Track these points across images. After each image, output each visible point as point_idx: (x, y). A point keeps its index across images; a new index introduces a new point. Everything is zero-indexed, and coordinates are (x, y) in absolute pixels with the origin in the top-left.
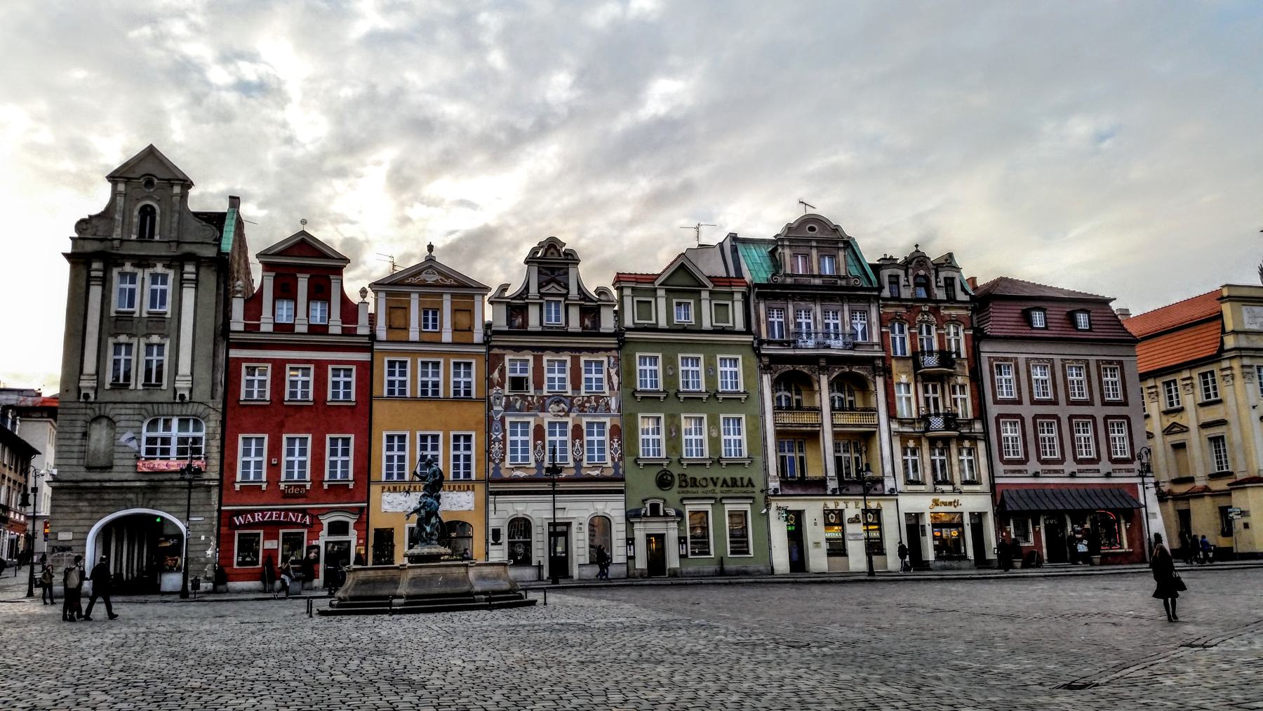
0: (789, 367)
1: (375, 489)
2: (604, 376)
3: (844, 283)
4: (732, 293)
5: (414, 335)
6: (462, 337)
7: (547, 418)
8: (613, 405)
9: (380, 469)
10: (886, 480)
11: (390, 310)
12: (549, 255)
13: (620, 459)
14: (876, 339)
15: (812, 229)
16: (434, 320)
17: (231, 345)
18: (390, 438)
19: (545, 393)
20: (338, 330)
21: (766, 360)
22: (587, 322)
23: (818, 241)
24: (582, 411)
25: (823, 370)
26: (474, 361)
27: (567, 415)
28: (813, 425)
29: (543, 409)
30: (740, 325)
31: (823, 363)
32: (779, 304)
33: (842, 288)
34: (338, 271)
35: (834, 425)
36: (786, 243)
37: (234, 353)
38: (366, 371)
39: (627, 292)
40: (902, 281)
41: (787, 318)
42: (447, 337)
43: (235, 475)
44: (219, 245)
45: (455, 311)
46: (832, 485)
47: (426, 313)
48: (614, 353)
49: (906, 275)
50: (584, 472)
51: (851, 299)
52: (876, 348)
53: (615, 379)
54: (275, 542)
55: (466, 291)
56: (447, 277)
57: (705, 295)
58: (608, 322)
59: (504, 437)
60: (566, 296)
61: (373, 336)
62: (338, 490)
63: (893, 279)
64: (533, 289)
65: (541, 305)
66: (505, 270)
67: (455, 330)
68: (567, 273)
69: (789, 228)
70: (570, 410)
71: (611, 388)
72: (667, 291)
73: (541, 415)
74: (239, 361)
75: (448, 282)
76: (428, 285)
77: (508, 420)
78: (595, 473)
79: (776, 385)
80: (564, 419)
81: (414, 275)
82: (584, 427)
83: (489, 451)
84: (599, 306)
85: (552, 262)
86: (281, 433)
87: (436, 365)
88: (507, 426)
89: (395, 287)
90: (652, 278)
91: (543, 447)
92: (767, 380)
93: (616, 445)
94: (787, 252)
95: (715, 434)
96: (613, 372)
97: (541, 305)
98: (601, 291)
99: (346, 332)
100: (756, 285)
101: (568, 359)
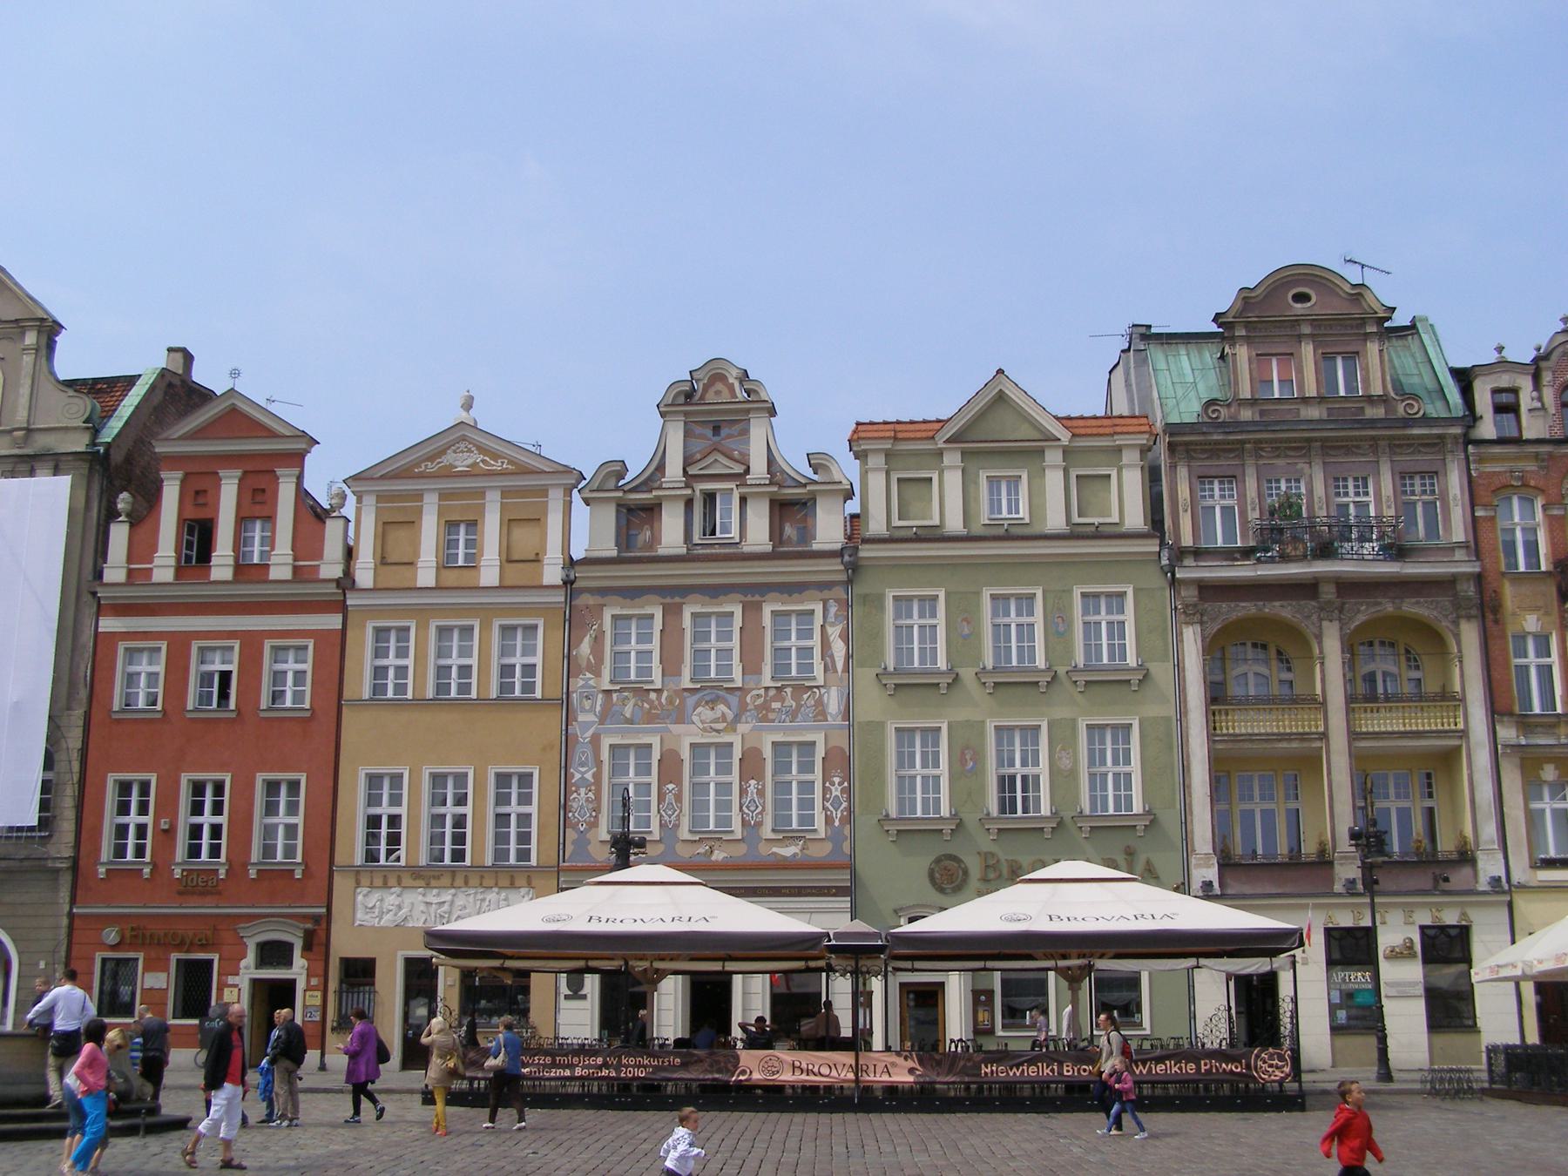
0: (1247, 608)
1: (341, 884)
2: (816, 641)
3: (1378, 412)
4: (1119, 450)
5: (426, 576)
6: (517, 574)
7: (686, 736)
8: (833, 702)
9: (352, 846)
10: (1480, 856)
11: (385, 528)
12: (710, 397)
13: (849, 817)
14: (1459, 533)
15: (1301, 298)
16: (470, 544)
17: (100, 611)
18: (374, 781)
19: (686, 683)
20: (285, 573)
21: (1190, 594)
22: (789, 531)
23: (1315, 323)
24: (765, 719)
25: (1326, 610)
26: (541, 623)
27: (731, 727)
28: (1302, 737)
29: (681, 718)
30: (1135, 518)
31: (1328, 593)
32: (1225, 463)
33: (1373, 423)
34: (296, 459)
35: (1353, 735)
36: (1240, 332)
37: (108, 624)
38: (334, 651)
39: (877, 461)
40: (1526, 399)
41: (1242, 497)
42: (489, 575)
43: (98, 850)
44: (96, 432)
45: (509, 523)
46: (1348, 871)
47: (452, 526)
48: (839, 592)
49: (1537, 384)
50: (764, 850)
51: (1397, 446)
52: (1460, 555)
53: (839, 649)
54: (163, 976)
55: (529, 482)
56: (496, 456)
57: (1054, 457)
58: (829, 529)
59: (598, 777)
60: (740, 478)
61: (347, 582)
62: (275, 879)
63: (1505, 398)
64: (674, 469)
65: (689, 503)
66: (626, 430)
67: (508, 559)
68: (745, 432)
69: (1246, 298)
70: (737, 719)
71: (829, 668)
72: (964, 453)
73: (676, 729)
74: (114, 637)
75: (497, 466)
76: (449, 473)
77: (606, 742)
78: (788, 851)
79: (1215, 650)
80: (726, 738)
81: (431, 458)
82: (768, 753)
83: (565, 807)
84: (813, 493)
85: (713, 407)
87: (467, 631)
88: (605, 755)
89: (396, 482)
90: (928, 429)
91: (679, 798)
92: (1191, 642)
93: (836, 791)
94: (1242, 353)
95: (1065, 763)
96: (834, 632)
97: (689, 503)
98: (818, 462)
99: (300, 574)
100: (1172, 429)
101: (738, 611)
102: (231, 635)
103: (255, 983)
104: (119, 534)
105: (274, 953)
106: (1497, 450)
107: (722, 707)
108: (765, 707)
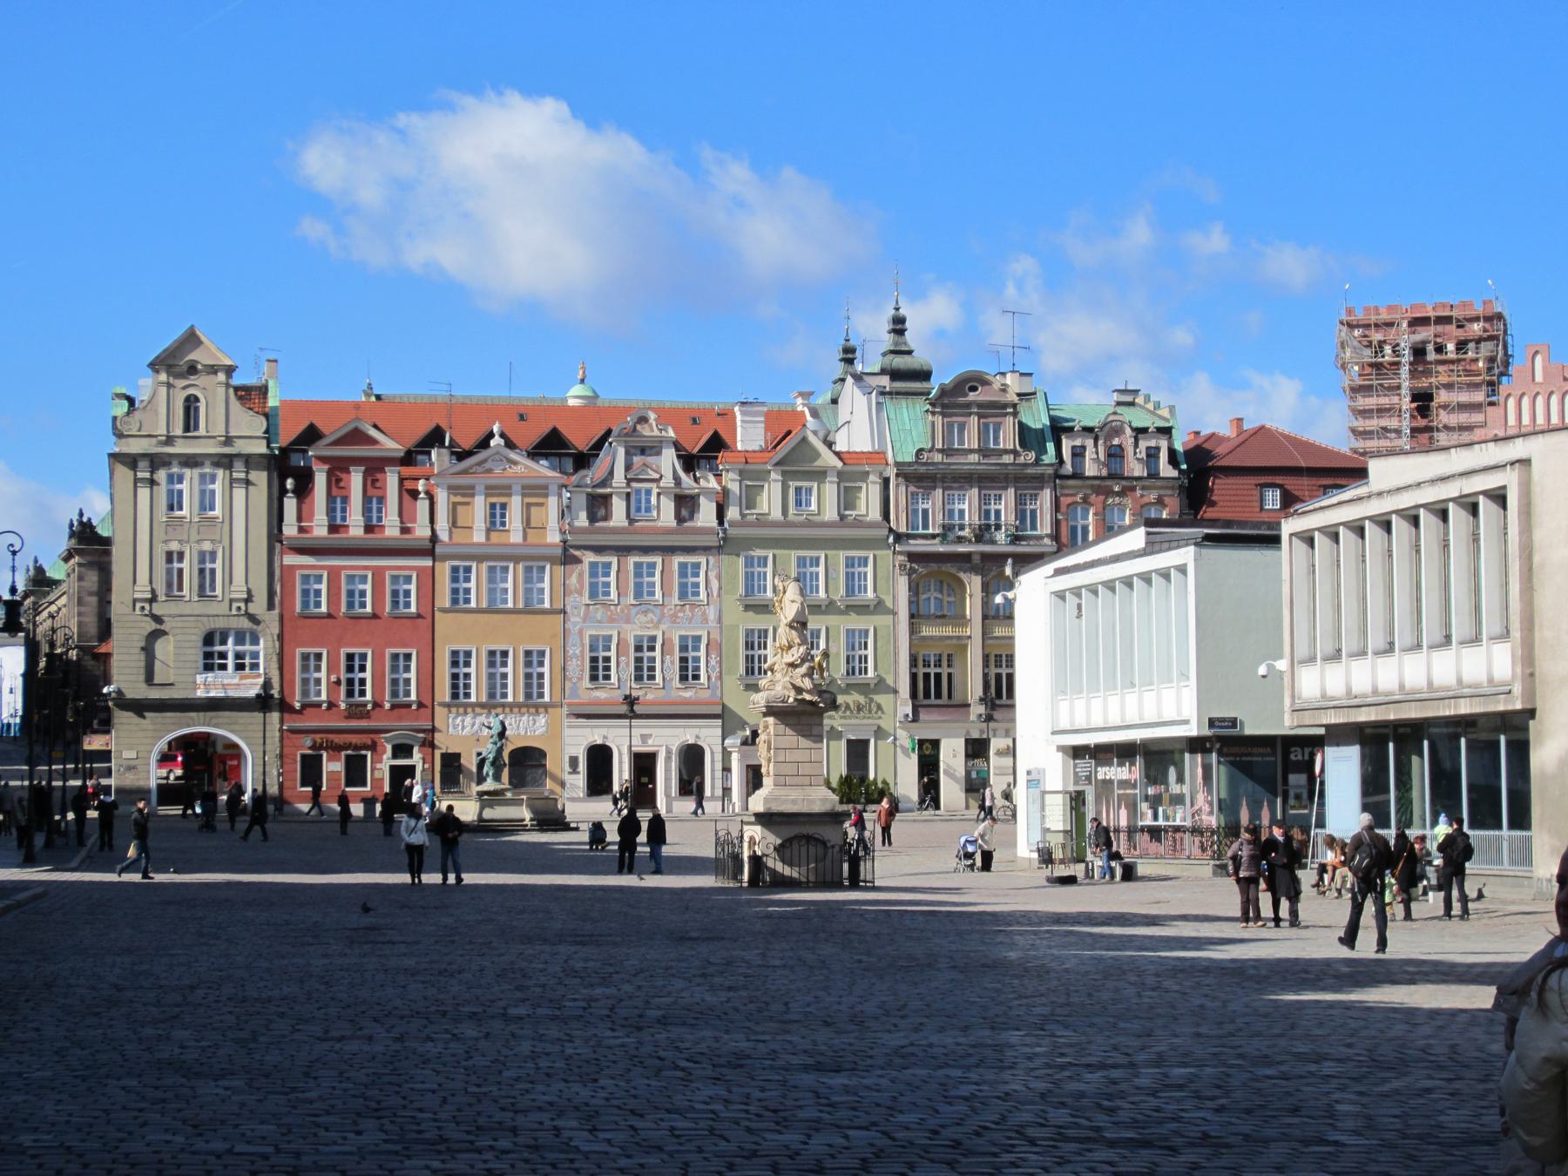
27: (656, 627)
29: (628, 621)
53: (715, 584)
59: (582, 652)
61: (434, 538)
65: (628, 495)
70: (659, 622)
72: (784, 473)
86: (339, 647)
102: (366, 568)
103: (392, 767)
104: (290, 504)
105: (402, 750)
106: (1071, 482)
107: (650, 615)
108: (675, 616)
